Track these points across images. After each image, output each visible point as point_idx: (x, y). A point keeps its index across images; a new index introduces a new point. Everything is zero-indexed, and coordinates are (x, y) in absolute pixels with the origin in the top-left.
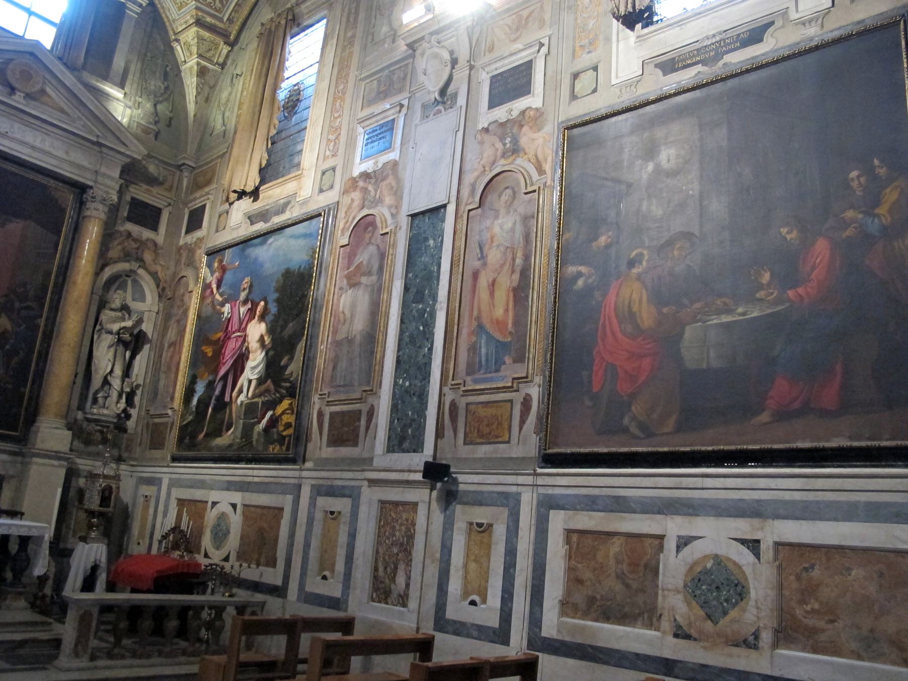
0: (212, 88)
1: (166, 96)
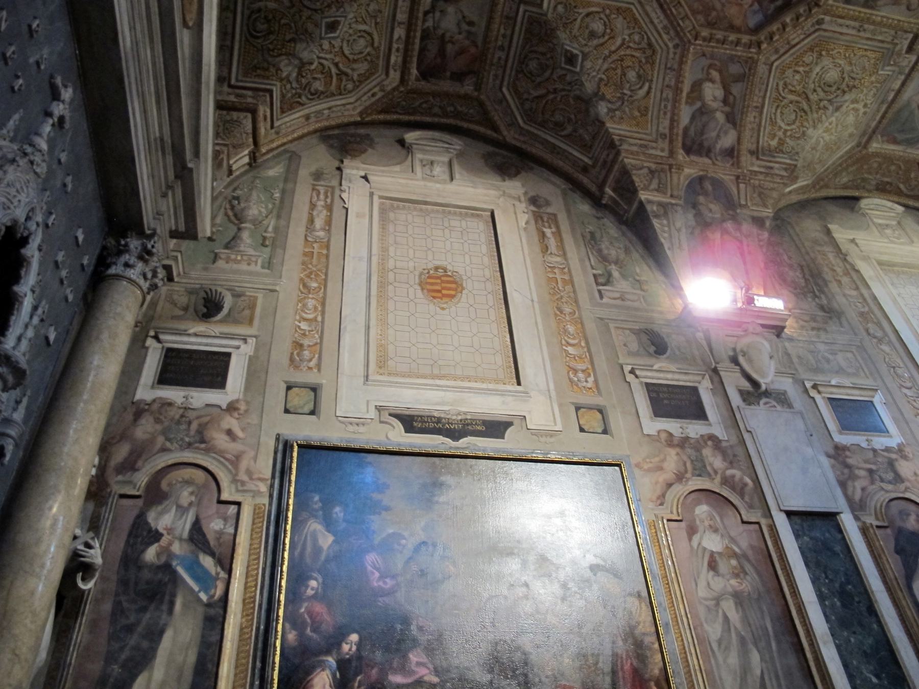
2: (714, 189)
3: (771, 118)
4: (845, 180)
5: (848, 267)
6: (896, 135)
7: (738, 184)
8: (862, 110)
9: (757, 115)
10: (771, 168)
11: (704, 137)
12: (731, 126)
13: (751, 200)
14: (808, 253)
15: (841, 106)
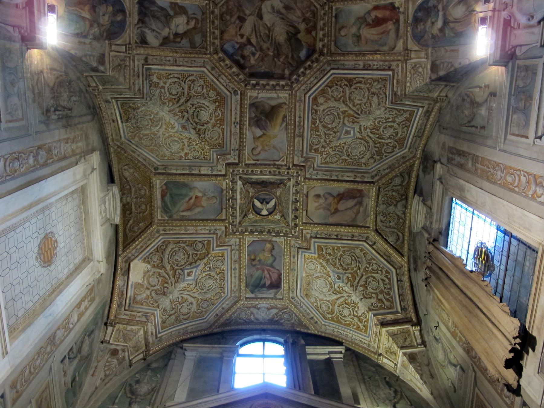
0: (429, 364)
1: (399, 397)
2: (118, 22)
3: (170, 74)
4: (127, 174)
5: (78, 157)
6: (168, 195)
7: (126, 45)
8: (182, 154)
9: (171, 62)
10: (139, 77)
11: (151, 18)
12: (161, 41)
13: (115, 56)
14: (79, 123)
15: (186, 129)
